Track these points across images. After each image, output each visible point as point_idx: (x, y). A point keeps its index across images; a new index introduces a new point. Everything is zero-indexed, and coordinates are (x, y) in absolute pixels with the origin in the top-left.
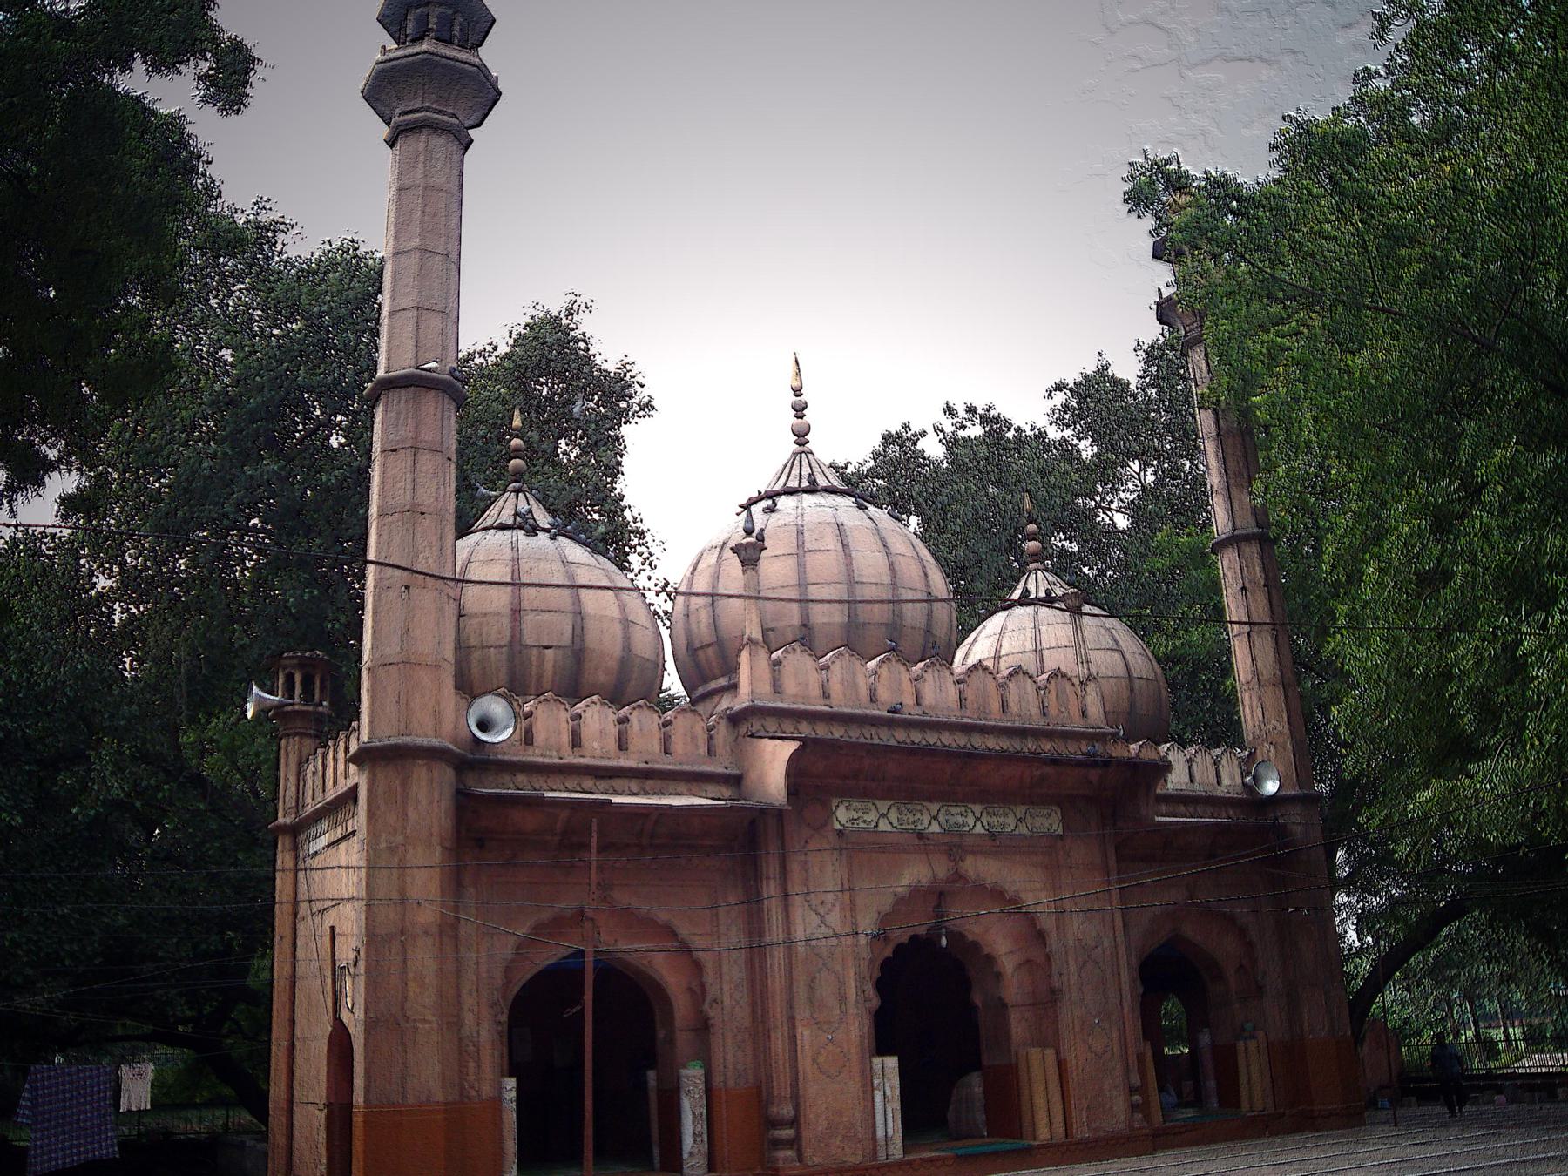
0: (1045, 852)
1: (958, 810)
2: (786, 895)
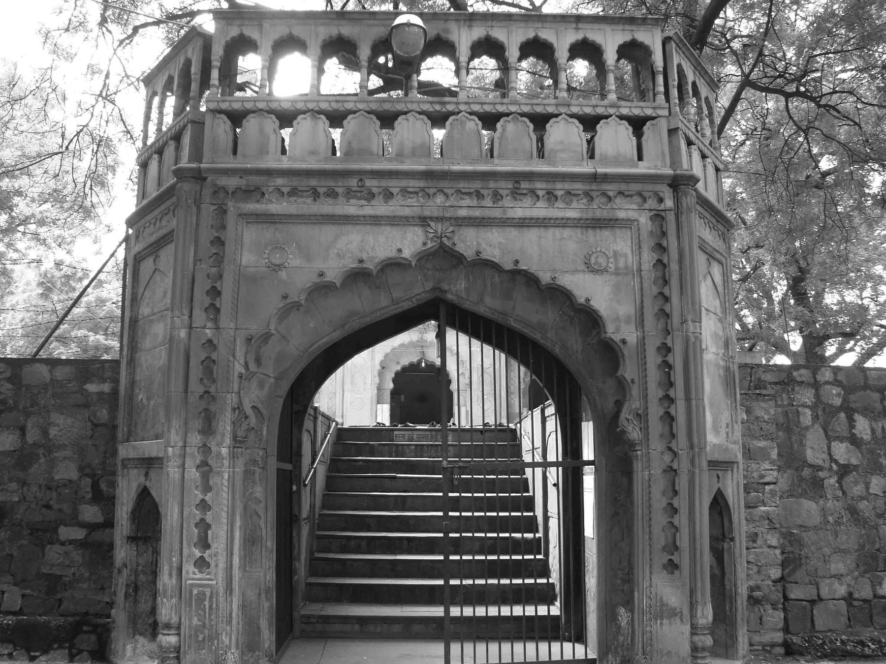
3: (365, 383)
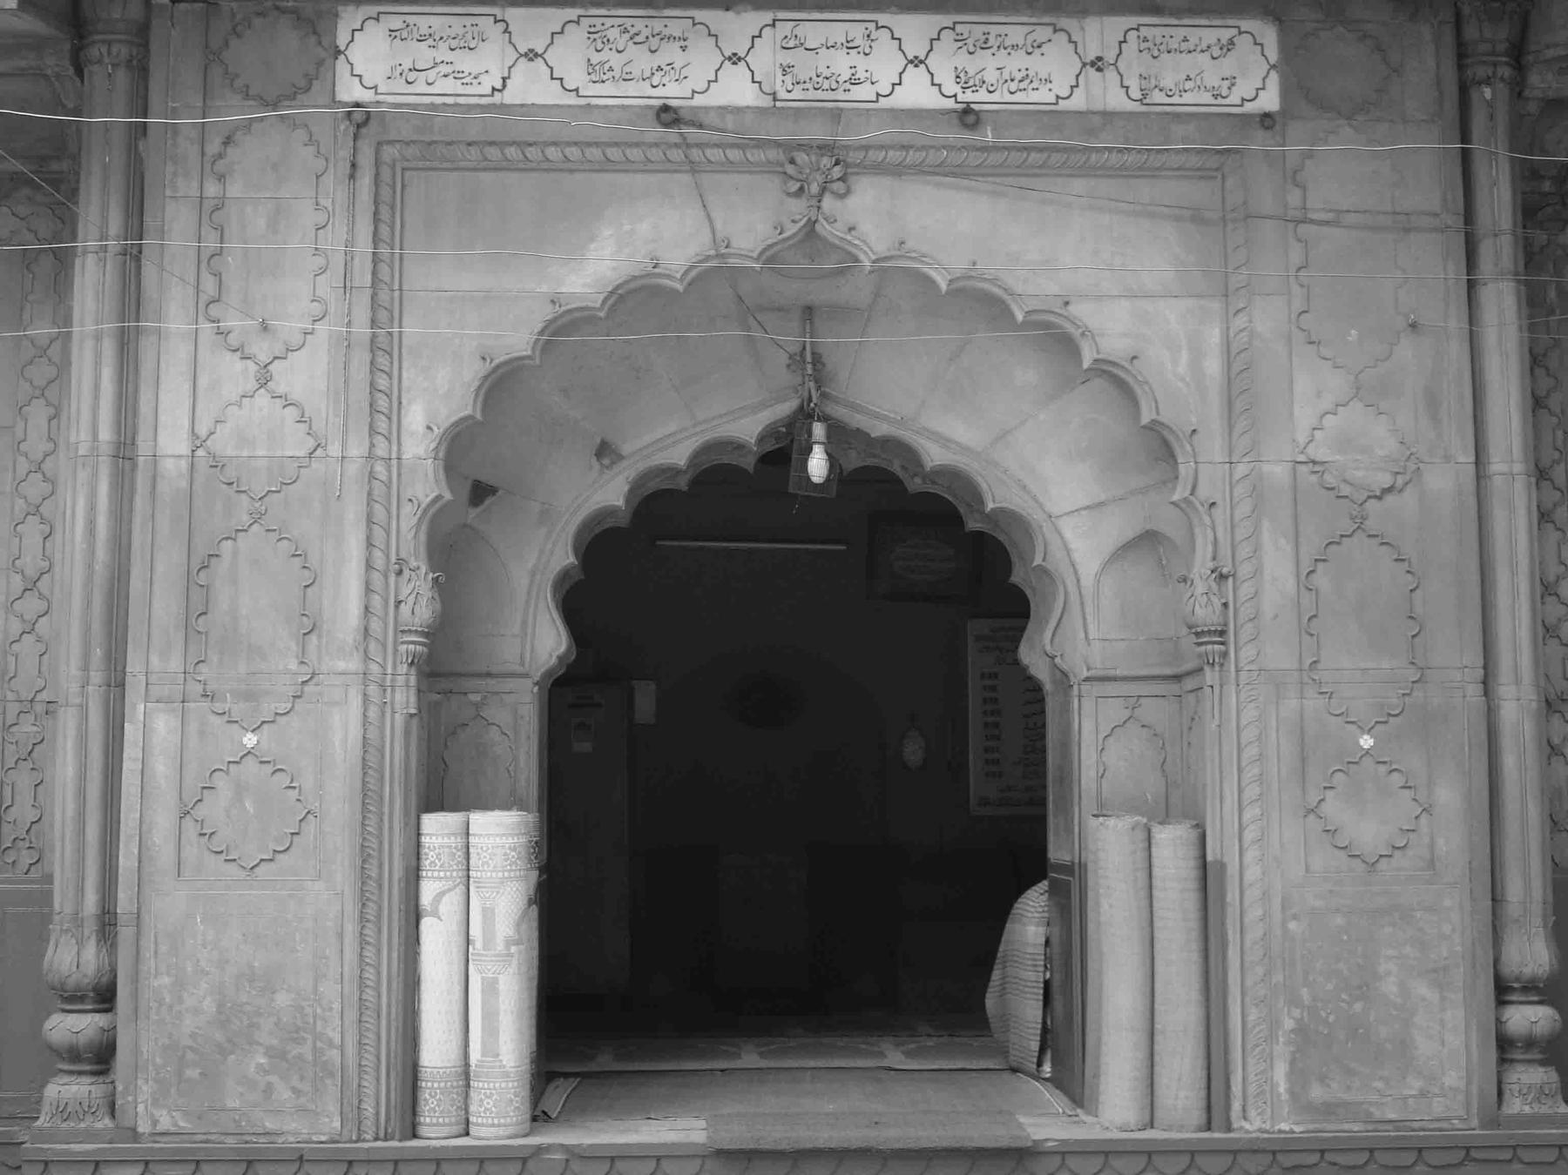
0: (1205, 173)
1: (837, 32)
2: (131, 300)
3: (310, 627)
